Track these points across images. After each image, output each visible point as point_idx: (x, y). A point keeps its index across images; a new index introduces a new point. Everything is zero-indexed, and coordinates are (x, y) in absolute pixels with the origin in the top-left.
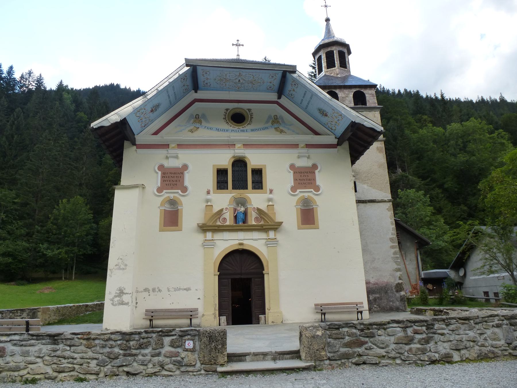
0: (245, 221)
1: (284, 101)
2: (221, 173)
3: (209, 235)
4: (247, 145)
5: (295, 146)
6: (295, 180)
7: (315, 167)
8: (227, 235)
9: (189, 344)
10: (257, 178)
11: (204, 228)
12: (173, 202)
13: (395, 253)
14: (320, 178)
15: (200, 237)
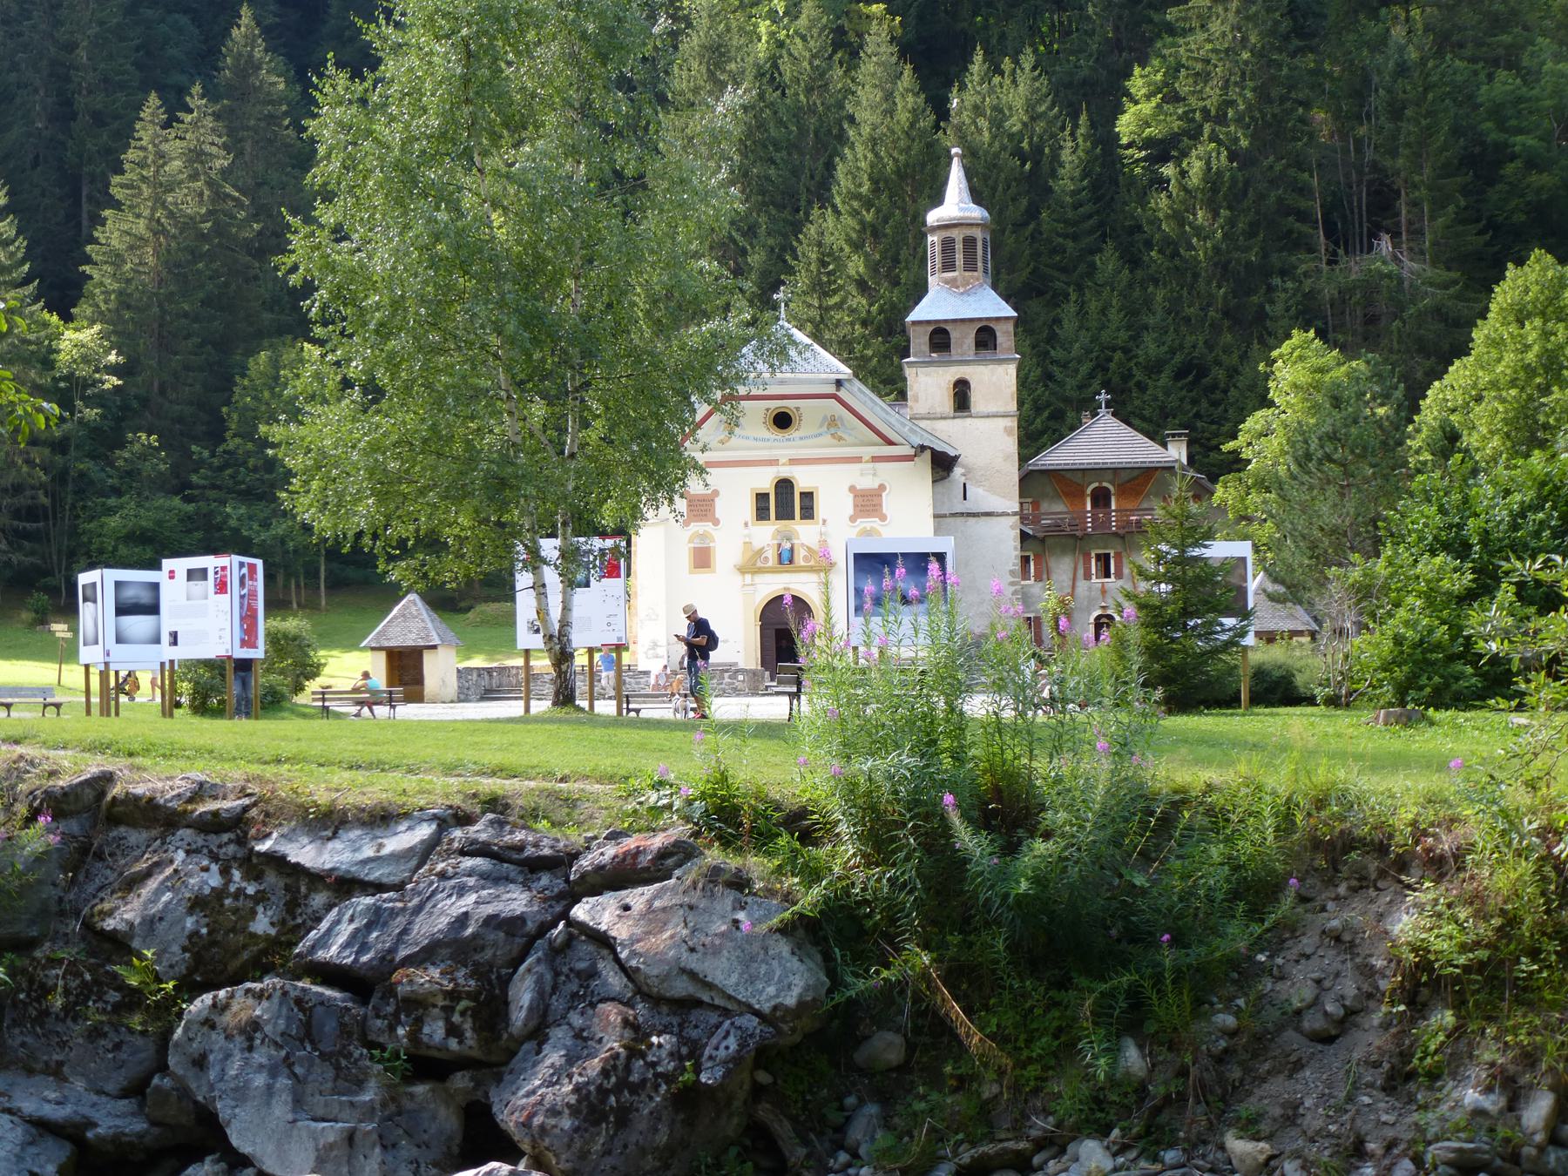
0: (791, 561)
1: (842, 394)
2: (762, 498)
3: (748, 577)
4: (793, 462)
5: (858, 460)
6: (856, 506)
7: (882, 487)
8: (768, 577)
9: (741, 677)
10: (806, 501)
11: (743, 570)
12: (703, 536)
13: (1015, 593)
14: (889, 503)
15: (738, 578)
